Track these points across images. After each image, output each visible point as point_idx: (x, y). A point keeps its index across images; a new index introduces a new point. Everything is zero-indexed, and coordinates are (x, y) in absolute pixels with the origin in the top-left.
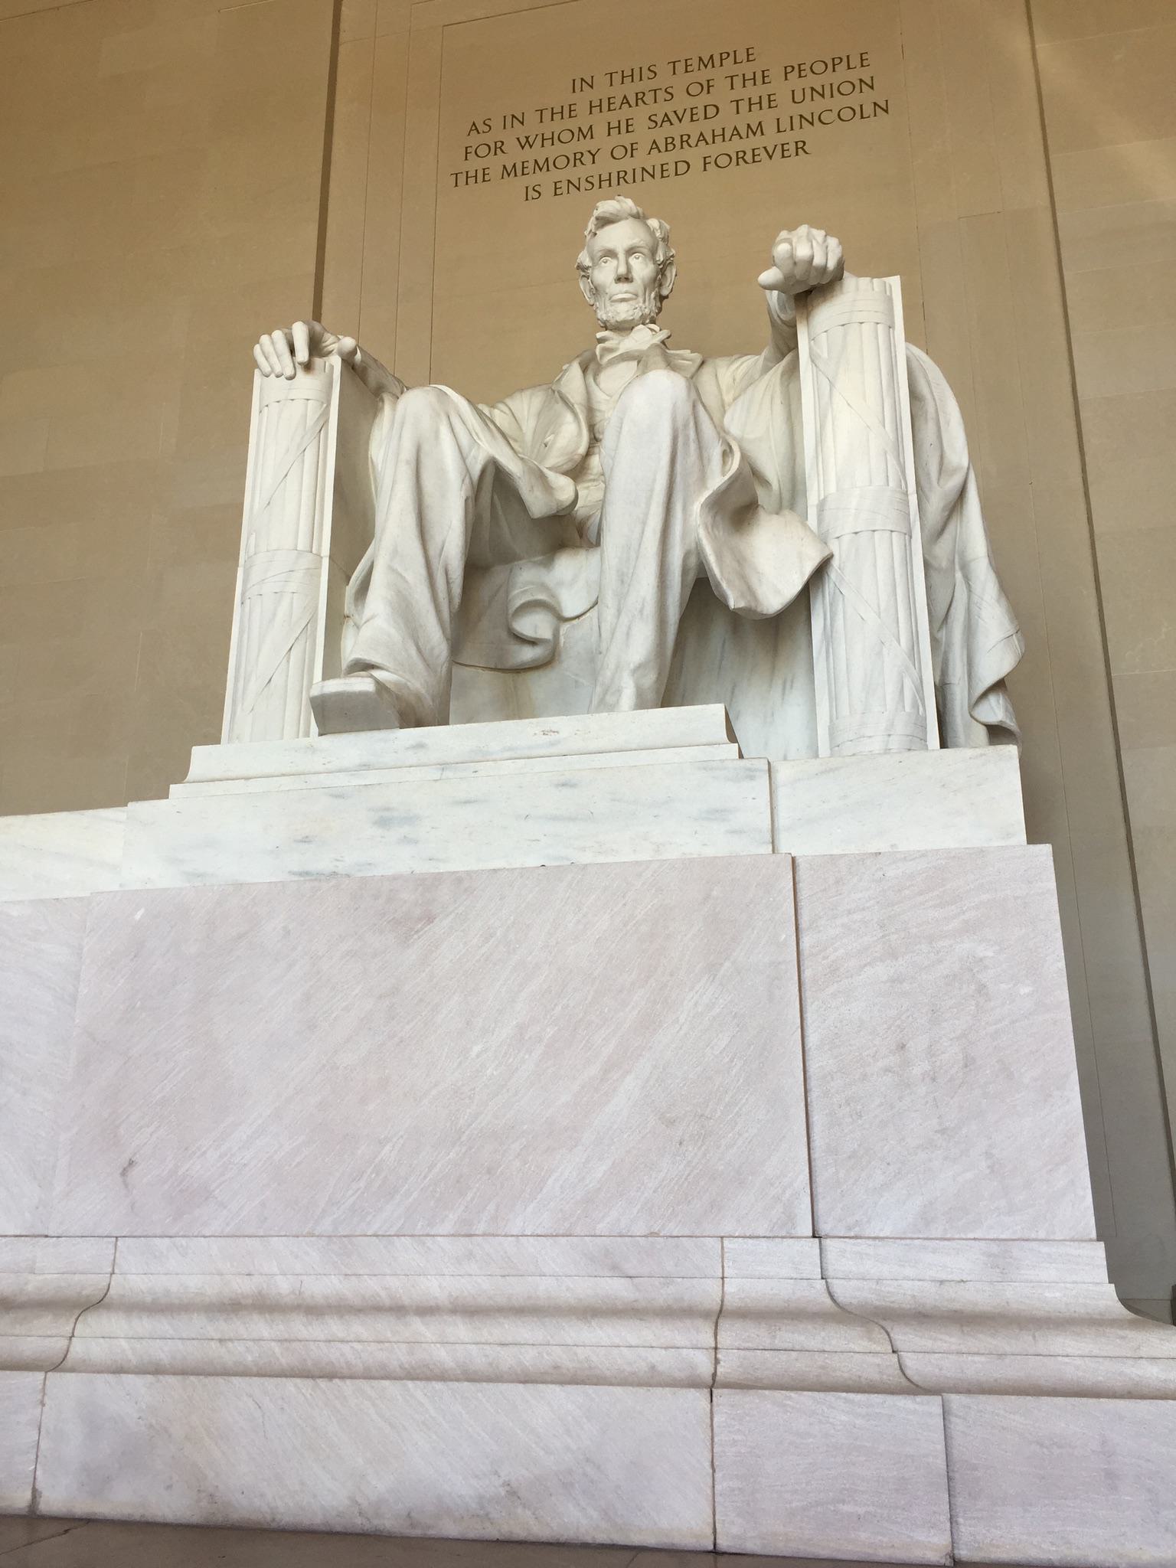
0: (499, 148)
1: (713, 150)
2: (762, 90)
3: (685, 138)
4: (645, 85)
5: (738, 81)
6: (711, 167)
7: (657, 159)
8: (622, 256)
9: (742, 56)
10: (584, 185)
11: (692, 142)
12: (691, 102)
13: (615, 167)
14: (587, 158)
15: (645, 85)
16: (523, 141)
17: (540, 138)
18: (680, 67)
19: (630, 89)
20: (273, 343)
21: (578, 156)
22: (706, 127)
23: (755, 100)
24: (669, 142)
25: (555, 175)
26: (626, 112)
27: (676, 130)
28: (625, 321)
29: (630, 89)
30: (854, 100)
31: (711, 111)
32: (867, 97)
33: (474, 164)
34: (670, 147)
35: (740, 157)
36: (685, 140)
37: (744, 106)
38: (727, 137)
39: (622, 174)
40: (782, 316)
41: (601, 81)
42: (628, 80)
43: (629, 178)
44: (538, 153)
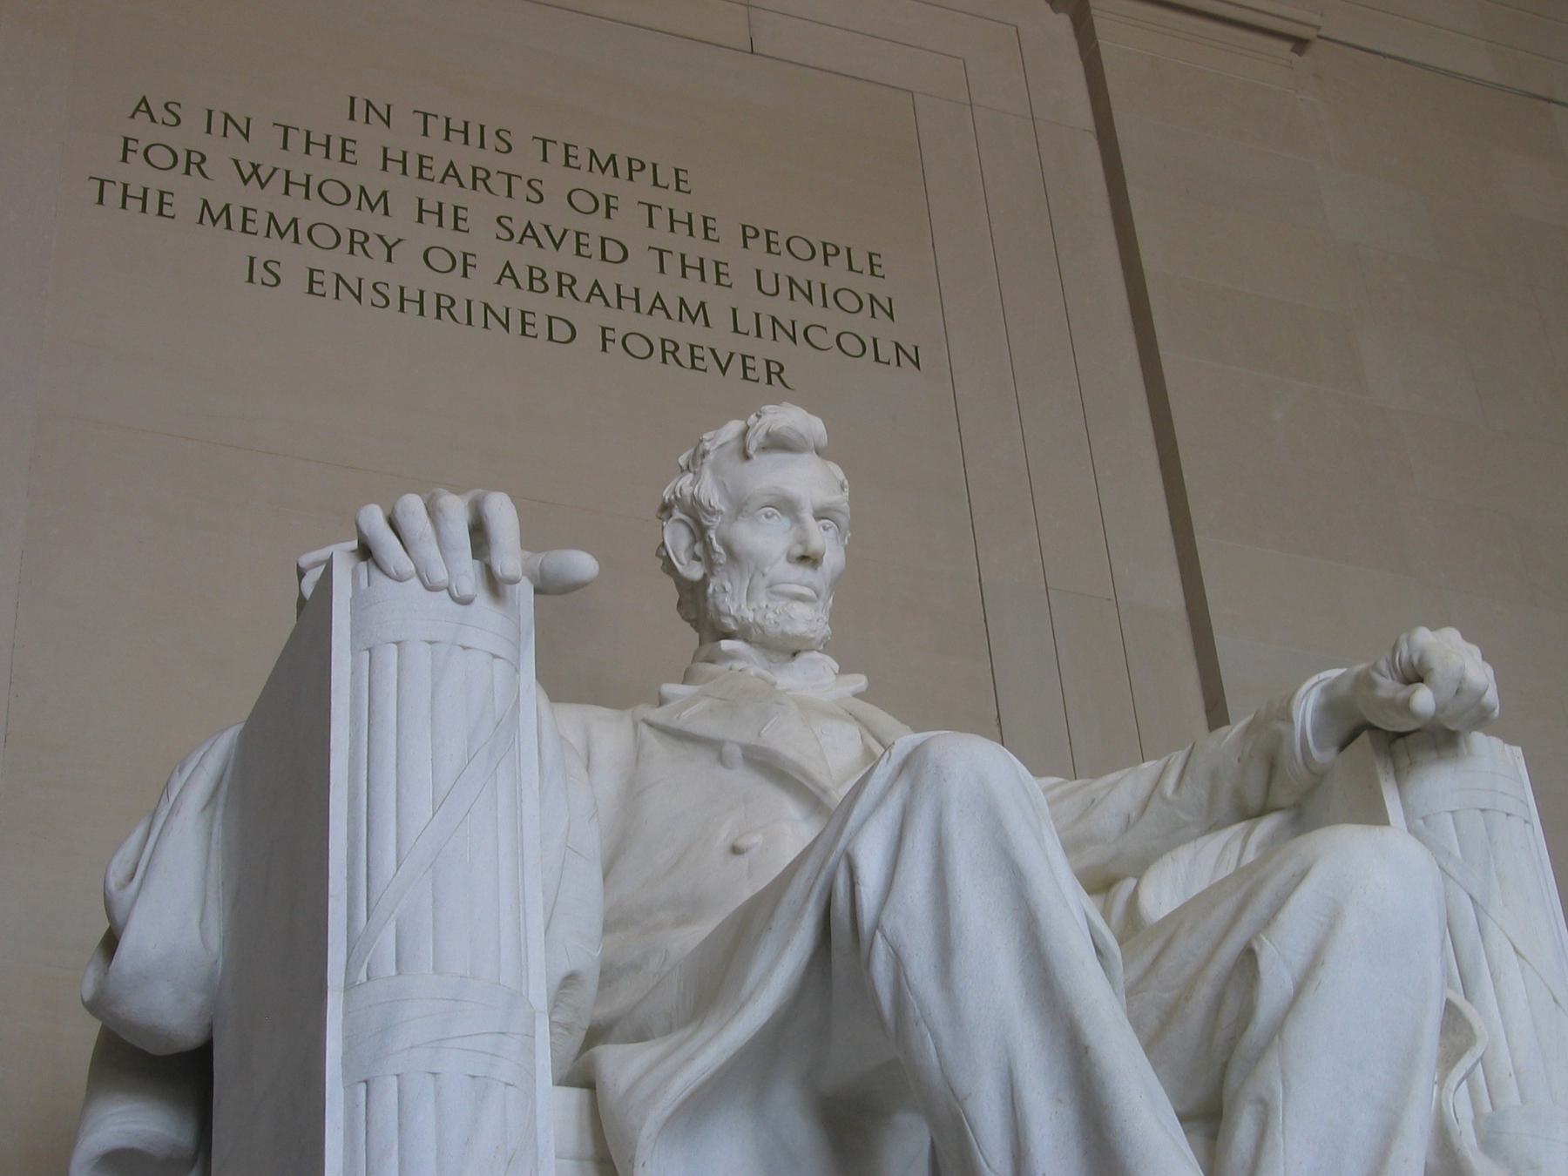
1: (623, 320)
2: (711, 253)
3: (566, 280)
4: (489, 159)
5: (661, 218)
6: (615, 348)
7: (510, 298)
9: (666, 177)
10: (368, 293)
11: (582, 289)
12: (576, 222)
13: (434, 284)
14: (375, 246)
15: (489, 159)
16: (247, 170)
17: (280, 175)
18: (556, 153)
19: (466, 157)
20: (433, 512)
21: (359, 237)
22: (609, 277)
23: (692, 261)
24: (536, 278)
25: (306, 255)
26: (450, 194)
27: (555, 261)
28: (800, 638)
29: (466, 157)
30: (865, 325)
31: (614, 252)
32: (881, 328)
33: (137, 174)
34: (538, 285)
35: (669, 351)
36: (566, 284)
37: (672, 263)
38: (645, 307)
39: (445, 302)
40: (1315, 754)
43: (460, 310)
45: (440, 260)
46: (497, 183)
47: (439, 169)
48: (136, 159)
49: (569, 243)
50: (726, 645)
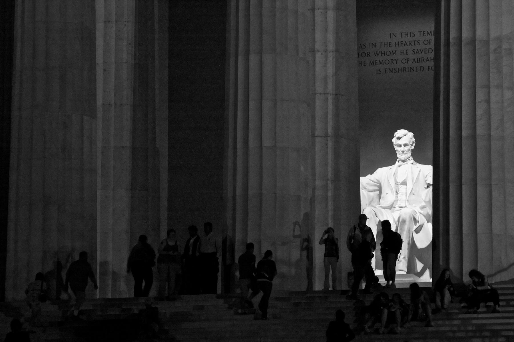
0: (369, 55)
8: (403, 146)
10: (394, 70)
14: (395, 62)
15: (412, 39)
16: (376, 53)
18: (422, 33)
24: (418, 59)
26: (406, 48)
27: (420, 56)
29: (407, 39)
36: (423, 60)
41: (399, 35)
42: (406, 36)
43: (407, 70)
44: (380, 58)
45: (404, 61)
46: (413, 43)
47: (404, 43)
48: (360, 56)
49: (423, 52)
50: (398, 160)
